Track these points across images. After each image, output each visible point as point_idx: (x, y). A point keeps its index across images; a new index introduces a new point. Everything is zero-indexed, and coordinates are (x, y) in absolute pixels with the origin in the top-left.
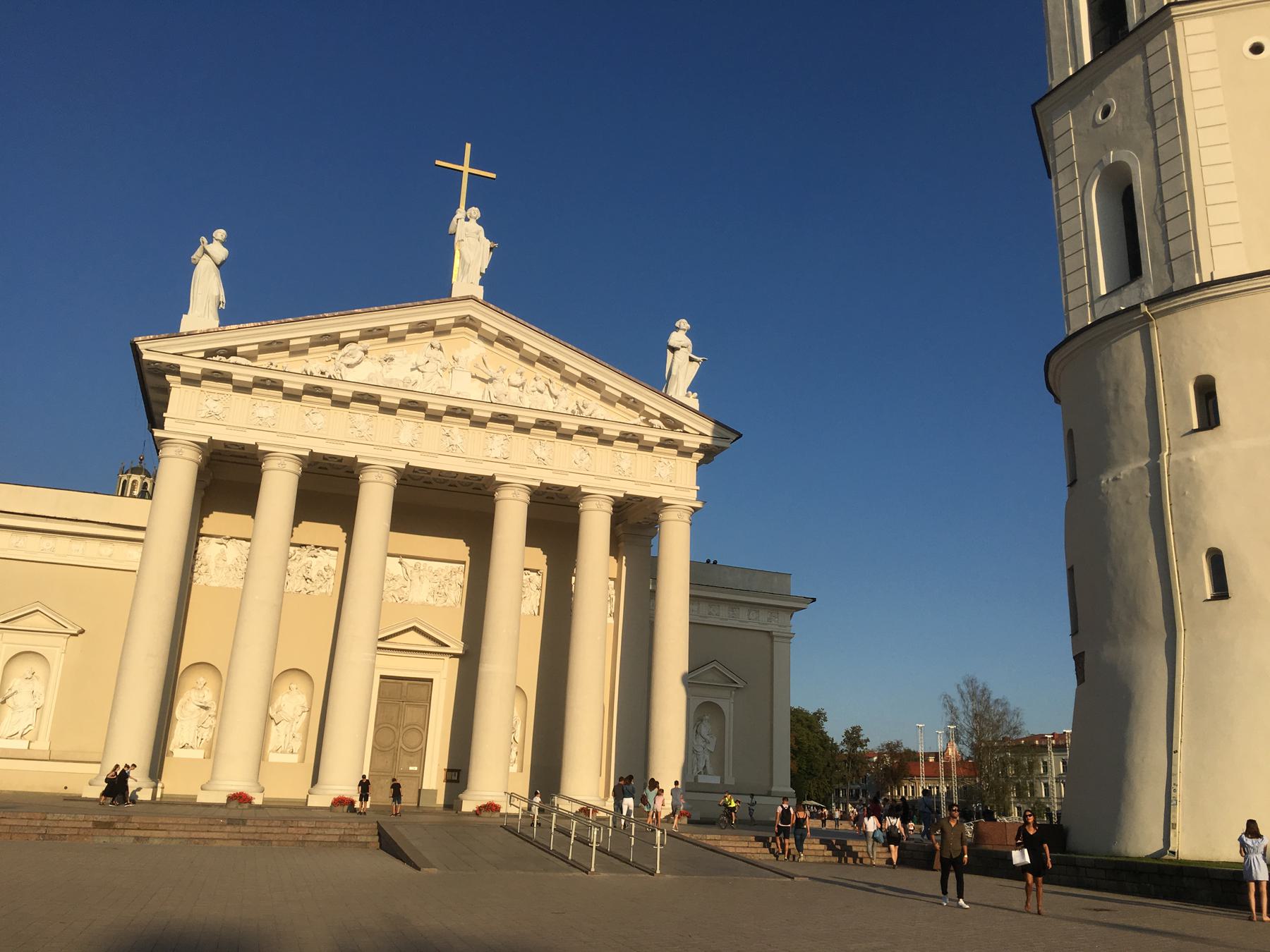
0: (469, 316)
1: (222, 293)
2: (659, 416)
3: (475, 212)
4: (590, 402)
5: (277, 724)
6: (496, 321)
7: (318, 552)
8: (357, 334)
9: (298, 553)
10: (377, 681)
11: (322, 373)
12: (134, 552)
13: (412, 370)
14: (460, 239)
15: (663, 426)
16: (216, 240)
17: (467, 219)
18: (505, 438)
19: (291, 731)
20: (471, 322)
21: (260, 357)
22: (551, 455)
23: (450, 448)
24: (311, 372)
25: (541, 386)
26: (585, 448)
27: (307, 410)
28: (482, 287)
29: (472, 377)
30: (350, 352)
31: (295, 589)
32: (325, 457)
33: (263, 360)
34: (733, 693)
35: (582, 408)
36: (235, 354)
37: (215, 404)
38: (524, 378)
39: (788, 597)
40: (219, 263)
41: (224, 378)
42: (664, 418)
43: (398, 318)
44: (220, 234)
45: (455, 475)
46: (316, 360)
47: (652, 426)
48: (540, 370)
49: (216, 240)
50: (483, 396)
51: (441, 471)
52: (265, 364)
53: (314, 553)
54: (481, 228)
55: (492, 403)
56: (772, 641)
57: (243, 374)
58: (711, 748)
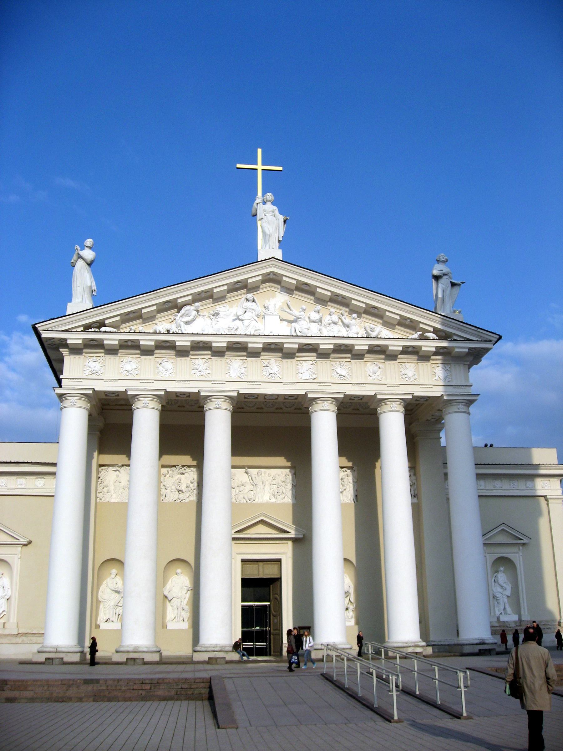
0: (272, 272)
1: (94, 284)
2: (431, 329)
3: (269, 196)
4: (376, 326)
5: (170, 601)
7: (185, 470)
8: (190, 298)
9: (170, 472)
10: (239, 564)
11: (168, 331)
13: (234, 320)
14: (260, 218)
15: (436, 338)
16: (87, 247)
17: (264, 203)
18: (312, 363)
19: (181, 605)
20: (275, 277)
21: (122, 326)
22: (350, 372)
23: (270, 376)
24: (159, 331)
25: (335, 318)
26: (376, 363)
27: (160, 361)
28: (281, 250)
29: (281, 320)
30: (187, 312)
31: (171, 499)
32: (177, 394)
33: (125, 327)
34: (521, 548)
35: (370, 332)
36: (104, 325)
37: (95, 364)
38: (321, 314)
40: (89, 262)
41: (97, 345)
45: (277, 397)
46: (163, 322)
47: (427, 339)
48: (332, 308)
49: (87, 247)
50: (291, 332)
51: (266, 395)
52: (127, 330)
53: (182, 470)
54: (275, 208)
55: (297, 336)
58: (508, 593)
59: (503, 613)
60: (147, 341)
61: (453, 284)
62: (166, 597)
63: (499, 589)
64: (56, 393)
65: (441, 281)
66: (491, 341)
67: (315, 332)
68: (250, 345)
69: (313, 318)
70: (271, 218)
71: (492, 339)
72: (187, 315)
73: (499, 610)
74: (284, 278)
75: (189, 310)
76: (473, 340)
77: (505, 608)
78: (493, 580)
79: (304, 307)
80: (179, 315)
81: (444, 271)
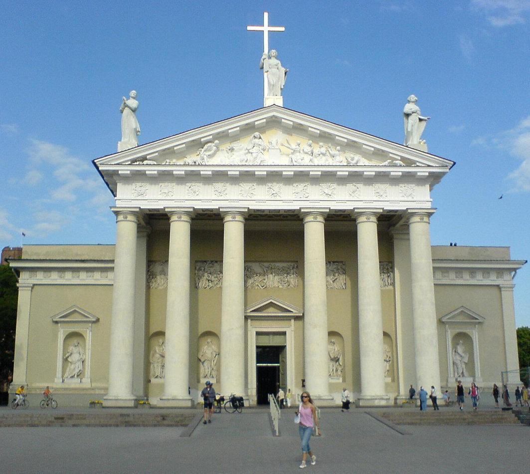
0: (274, 115)
2: (399, 158)
5: (203, 363)
6: (290, 118)
8: (211, 137)
12: (110, 275)
13: (245, 154)
15: (401, 163)
17: (270, 58)
20: (276, 119)
25: (323, 150)
28: (282, 97)
30: (209, 148)
34: (477, 326)
36: (146, 159)
37: (140, 189)
39: (508, 261)
42: (403, 159)
43: (233, 126)
44: (133, 93)
53: (211, 265)
56: (500, 291)
57: (152, 170)
59: (461, 376)
60: (179, 171)
61: (420, 120)
62: (200, 360)
63: (459, 358)
64: (113, 211)
65: (410, 118)
66: (447, 166)
67: (307, 161)
68: (256, 173)
69: (306, 150)
70: (274, 70)
71: (448, 165)
72: (210, 150)
73: (458, 374)
74: (283, 120)
75: (210, 146)
76: (432, 166)
77: (463, 373)
78: (454, 350)
79: (299, 142)
80: (203, 150)
81: (413, 110)
